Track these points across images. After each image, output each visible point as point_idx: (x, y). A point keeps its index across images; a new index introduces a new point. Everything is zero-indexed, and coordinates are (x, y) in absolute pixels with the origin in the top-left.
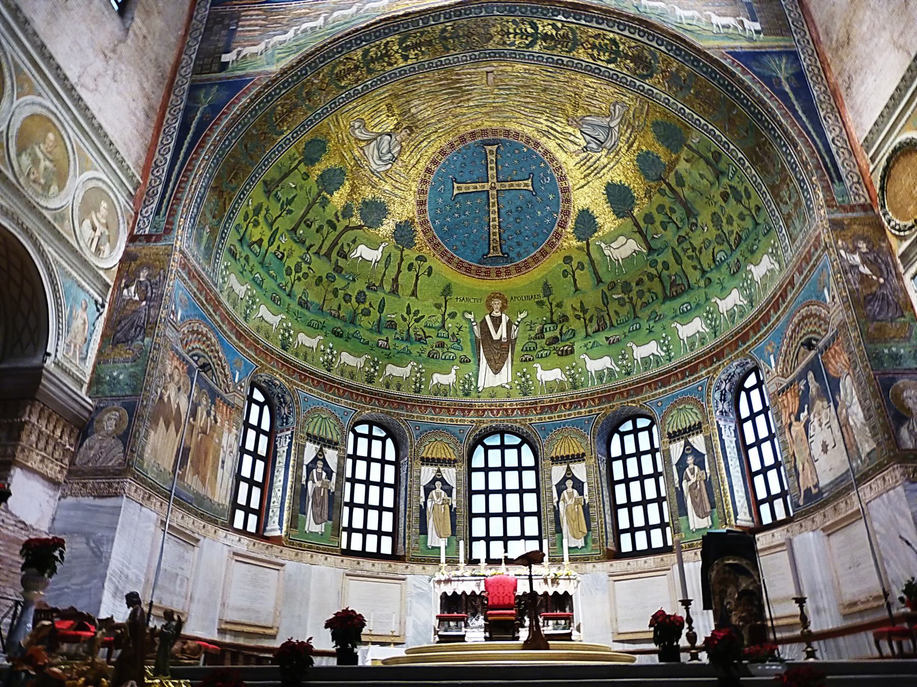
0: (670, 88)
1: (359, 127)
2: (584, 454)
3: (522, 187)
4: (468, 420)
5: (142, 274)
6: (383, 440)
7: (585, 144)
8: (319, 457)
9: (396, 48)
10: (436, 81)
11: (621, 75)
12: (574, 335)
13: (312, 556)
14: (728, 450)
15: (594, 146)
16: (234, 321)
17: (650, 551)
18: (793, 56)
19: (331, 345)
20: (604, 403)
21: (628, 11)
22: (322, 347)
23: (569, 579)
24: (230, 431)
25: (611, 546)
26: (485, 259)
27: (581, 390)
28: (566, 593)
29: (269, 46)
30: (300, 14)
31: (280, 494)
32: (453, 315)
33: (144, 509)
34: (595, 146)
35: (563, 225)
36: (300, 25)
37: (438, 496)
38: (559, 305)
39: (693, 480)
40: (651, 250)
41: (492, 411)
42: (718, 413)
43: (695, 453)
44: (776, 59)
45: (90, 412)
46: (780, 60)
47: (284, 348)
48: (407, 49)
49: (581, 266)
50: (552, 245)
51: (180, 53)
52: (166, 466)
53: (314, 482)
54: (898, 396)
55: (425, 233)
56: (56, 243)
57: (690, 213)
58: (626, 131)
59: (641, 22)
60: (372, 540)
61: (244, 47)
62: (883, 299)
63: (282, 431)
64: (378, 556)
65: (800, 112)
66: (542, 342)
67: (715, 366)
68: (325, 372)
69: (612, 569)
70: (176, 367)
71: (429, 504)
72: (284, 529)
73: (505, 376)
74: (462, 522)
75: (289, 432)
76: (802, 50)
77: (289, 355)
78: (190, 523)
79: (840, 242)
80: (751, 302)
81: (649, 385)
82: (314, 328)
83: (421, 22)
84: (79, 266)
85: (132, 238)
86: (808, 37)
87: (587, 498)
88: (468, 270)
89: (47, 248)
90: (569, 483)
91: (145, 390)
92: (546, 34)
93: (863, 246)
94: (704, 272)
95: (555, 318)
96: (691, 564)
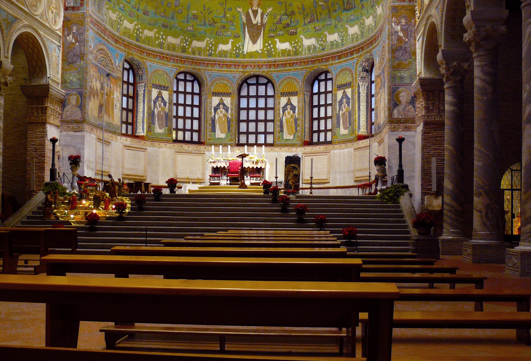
2: (297, 92)
5: (74, 29)
6: (192, 82)
8: (160, 96)
12: (298, 23)
13: (159, 144)
14: (361, 97)
16: (113, 34)
19: (162, 33)
20: (310, 64)
22: (157, 35)
23: (263, 162)
24: (117, 90)
25: (307, 139)
28: (261, 167)
31: (141, 115)
32: (230, 9)
33: (92, 135)
37: (221, 112)
39: (344, 110)
41: (251, 66)
42: (359, 78)
45: (64, 96)
47: (137, 41)
52: (96, 115)
53: (157, 109)
54: (397, 96)
56: (43, 28)
62: (405, 49)
63: (140, 83)
66: (280, 26)
67: (360, 54)
68: (159, 50)
69: (305, 151)
70: (94, 71)
71: (216, 117)
72: (145, 132)
73: (258, 46)
75: (143, 84)
78: (107, 136)
79: (393, 19)
80: (375, 25)
81: (332, 57)
84: (51, 34)
85: (66, 9)
87: (297, 115)
89: (41, 32)
90: (289, 107)
91: (85, 86)
93: (403, 21)
95: (288, 12)
96: (338, 151)
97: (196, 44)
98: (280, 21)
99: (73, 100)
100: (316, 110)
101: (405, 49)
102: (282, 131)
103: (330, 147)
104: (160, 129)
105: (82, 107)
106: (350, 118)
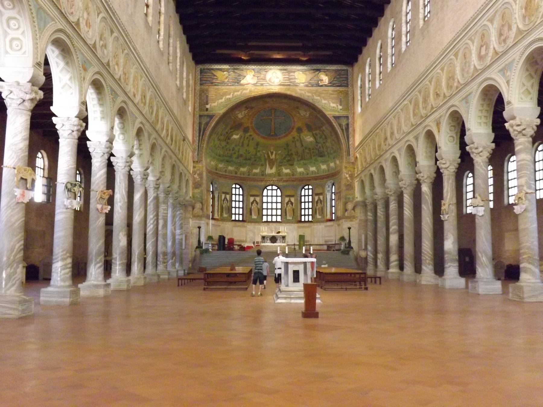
4: (263, 184)
8: (225, 198)
17: (308, 221)
18: (347, 117)
26: (269, 135)
27: (294, 177)
31: (217, 208)
32: (259, 151)
35: (293, 129)
36: (226, 96)
38: (291, 150)
40: (316, 142)
43: (320, 200)
47: (216, 170)
49: (298, 140)
50: (289, 133)
51: (195, 103)
55: (252, 129)
57: (326, 138)
59: (313, 104)
60: (237, 216)
64: (239, 221)
65: (345, 136)
66: (285, 160)
68: (224, 173)
71: (252, 207)
73: (273, 171)
74: (261, 211)
77: (217, 172)
82: (222, 161)
85: (194, 162)
88: (264, 138)
90: (290, 203)
93: (350, 173)
94: (328, 153)
97: (242, 169)
98: (285, 158)
99: (198, 205)
100: (303, 204)
101: (351, 185)
102: (286, 215)
103: (312, 224)
104: (226, 214)
105: (202, 209)
106: (322, 211)
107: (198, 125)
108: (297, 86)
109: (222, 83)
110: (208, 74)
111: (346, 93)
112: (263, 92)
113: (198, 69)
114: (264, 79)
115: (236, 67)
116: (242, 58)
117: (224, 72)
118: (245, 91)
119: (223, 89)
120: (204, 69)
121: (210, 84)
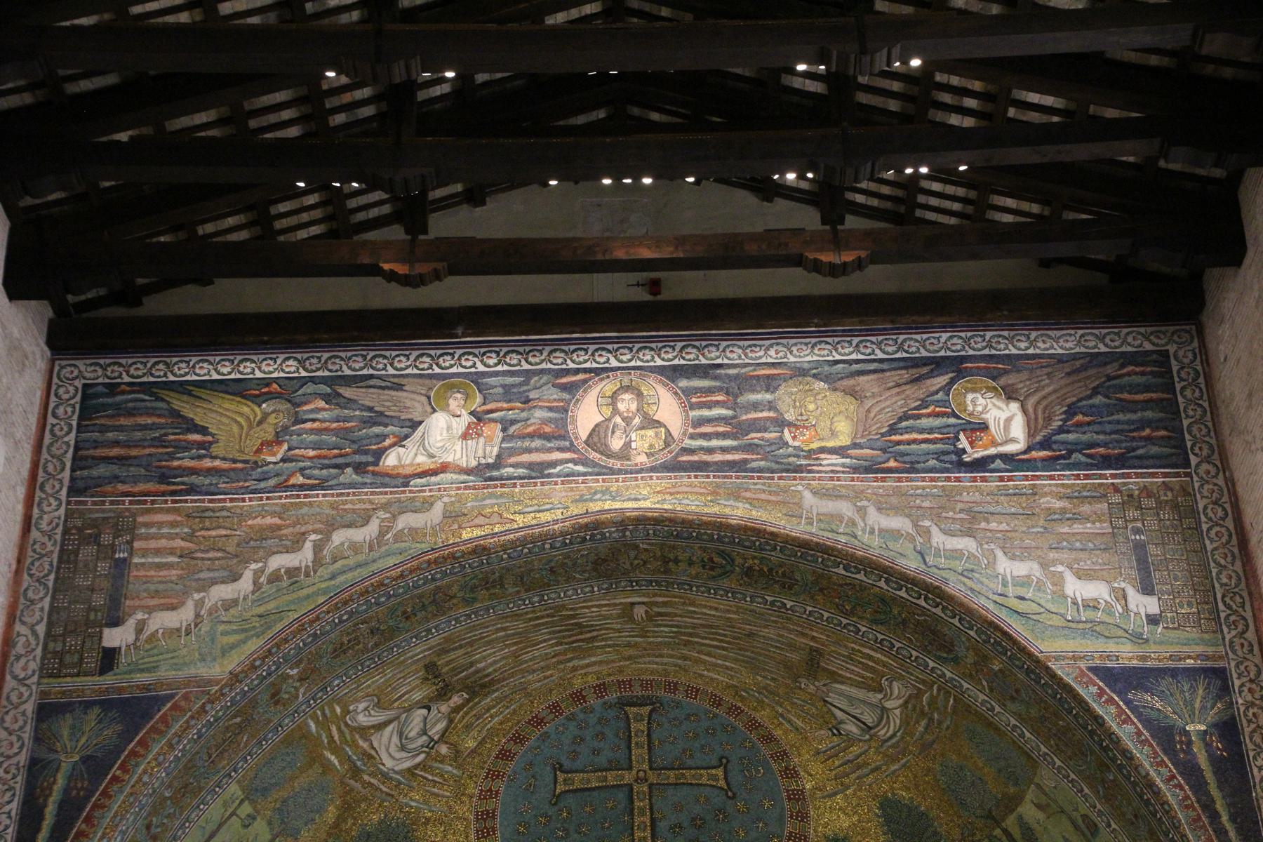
0: (991, 690)
1: (366, 709)
3: (704, 781)
7: (834, 722)
9: (455, 588)
10: (530, 620)
11: (898, 645)
15: (852, 728)
21: (903, 562)
29: (202, 613)
30: (262, 529)
34: (854, 729)
36: (265, 560)
44: (1186, 687)
46: (1193, 690)
48: (473, 589)
51: (11, 619)
58: (917, 722)
61: (150, 610)
65: (1225, 818)
76: (1237, 666)
83: (505, 556)
86: (1251, 635)
92: (750, 568)
107: (19, 784)
108: (798, 469)
109: (244, 474)
110: (141, 420)
111: (1175, 506)
112: (546, 517)
113: (70, 393)
114: (559, 434)
115: (351, 363)
116: (386, 267)
117: (258, 399)
118: (407, 521)
119: (242, 517)
120: (113, 388)
121: (151, 486)
